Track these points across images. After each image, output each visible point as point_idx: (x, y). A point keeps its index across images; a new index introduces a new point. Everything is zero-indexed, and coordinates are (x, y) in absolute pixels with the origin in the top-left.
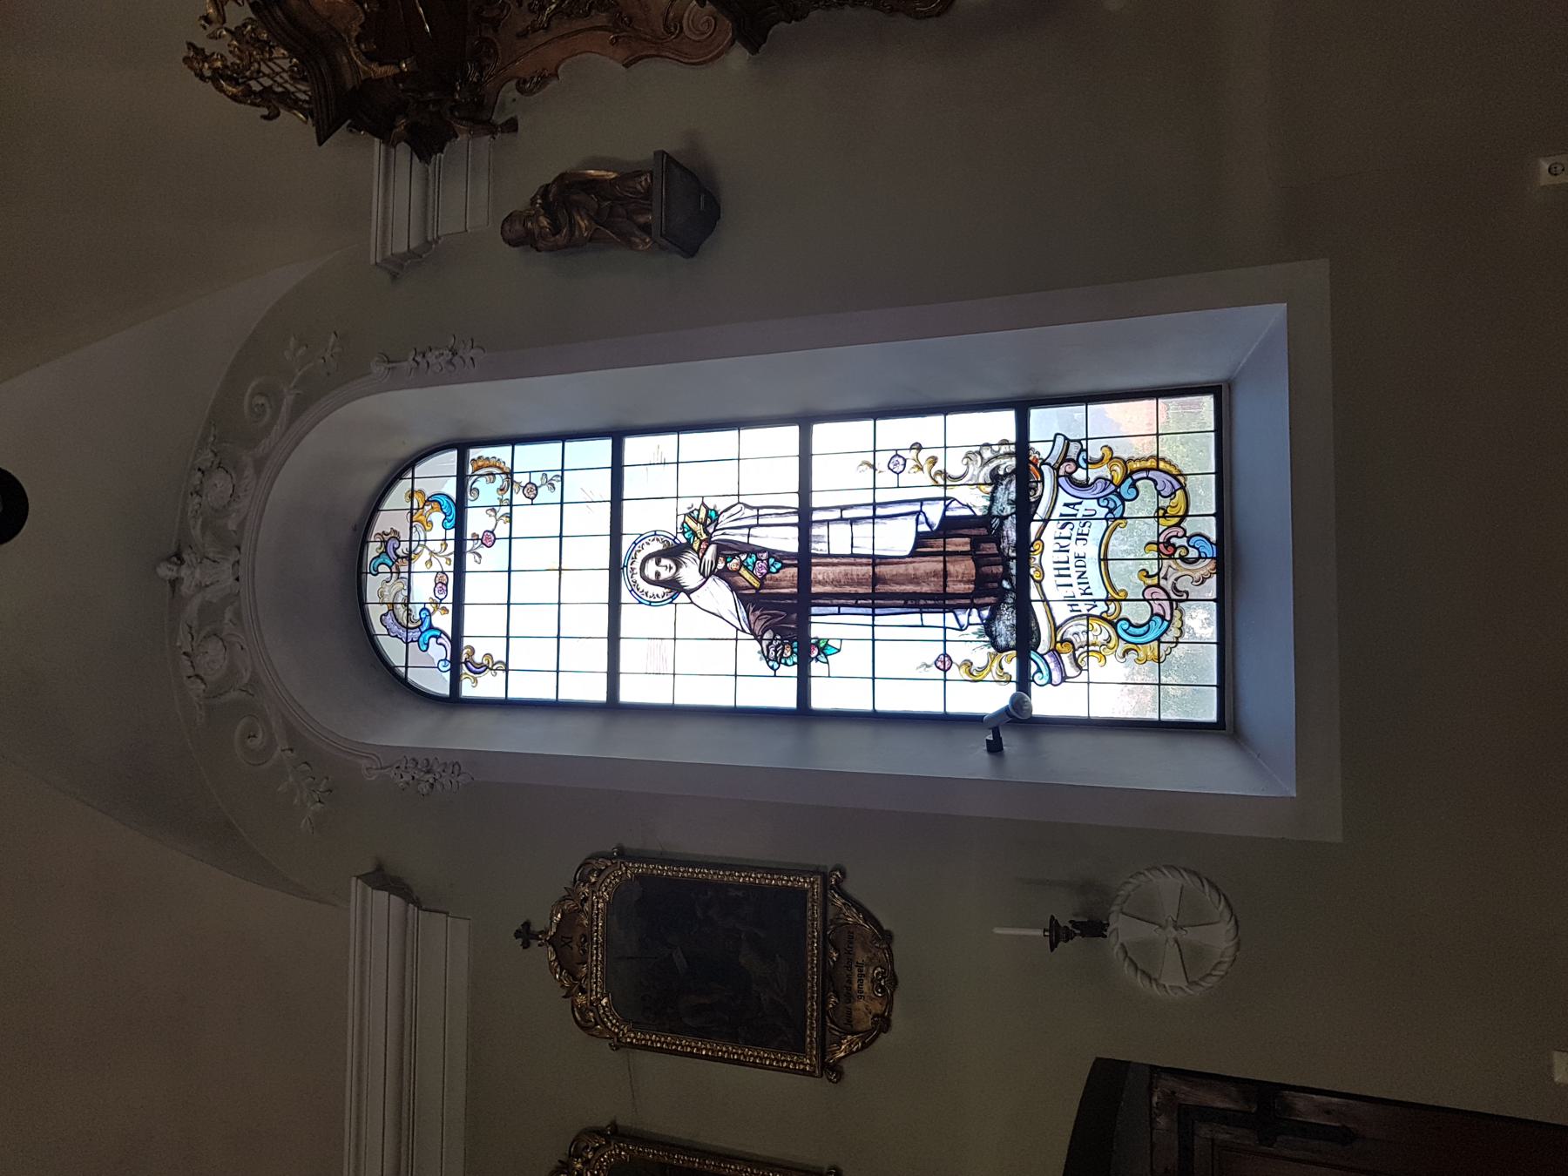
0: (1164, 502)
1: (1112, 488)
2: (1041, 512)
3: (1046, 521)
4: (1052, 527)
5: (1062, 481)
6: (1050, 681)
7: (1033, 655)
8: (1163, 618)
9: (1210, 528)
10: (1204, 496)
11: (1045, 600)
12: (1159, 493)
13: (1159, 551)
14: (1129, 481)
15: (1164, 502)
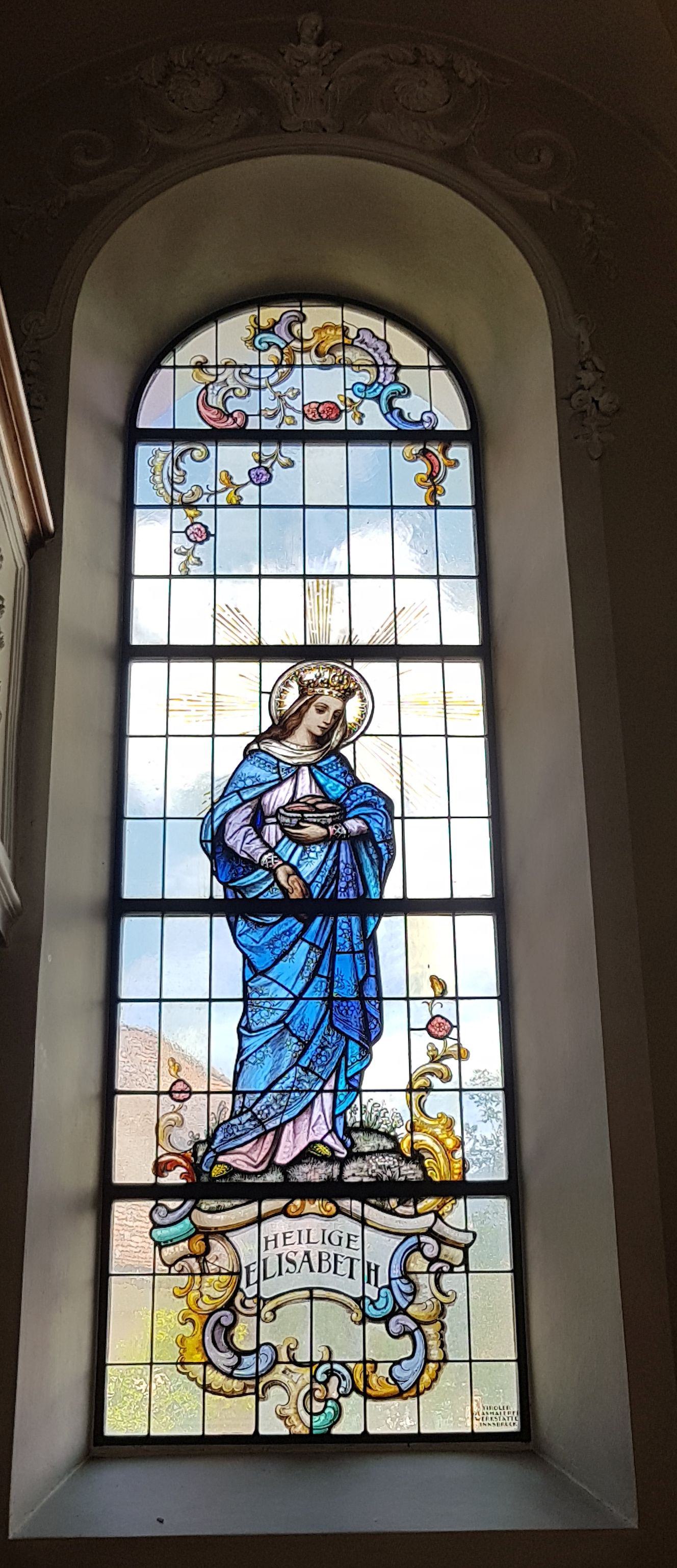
0: (383, 1370)
1: (404, 1305)
2: (371, 1213)
3: (363, 1221)
4: (356, 1228)
5: (414, 1240)
6: (156, 1226)
7: (189, 1204)
8: (234, 1368)
9: (349, 1426)
10: (392, 1419)
11: (259, 1219)
12: (398, 1362)
13: (321, 1363)
14: (412, 1326)
15: (383, 1370)
